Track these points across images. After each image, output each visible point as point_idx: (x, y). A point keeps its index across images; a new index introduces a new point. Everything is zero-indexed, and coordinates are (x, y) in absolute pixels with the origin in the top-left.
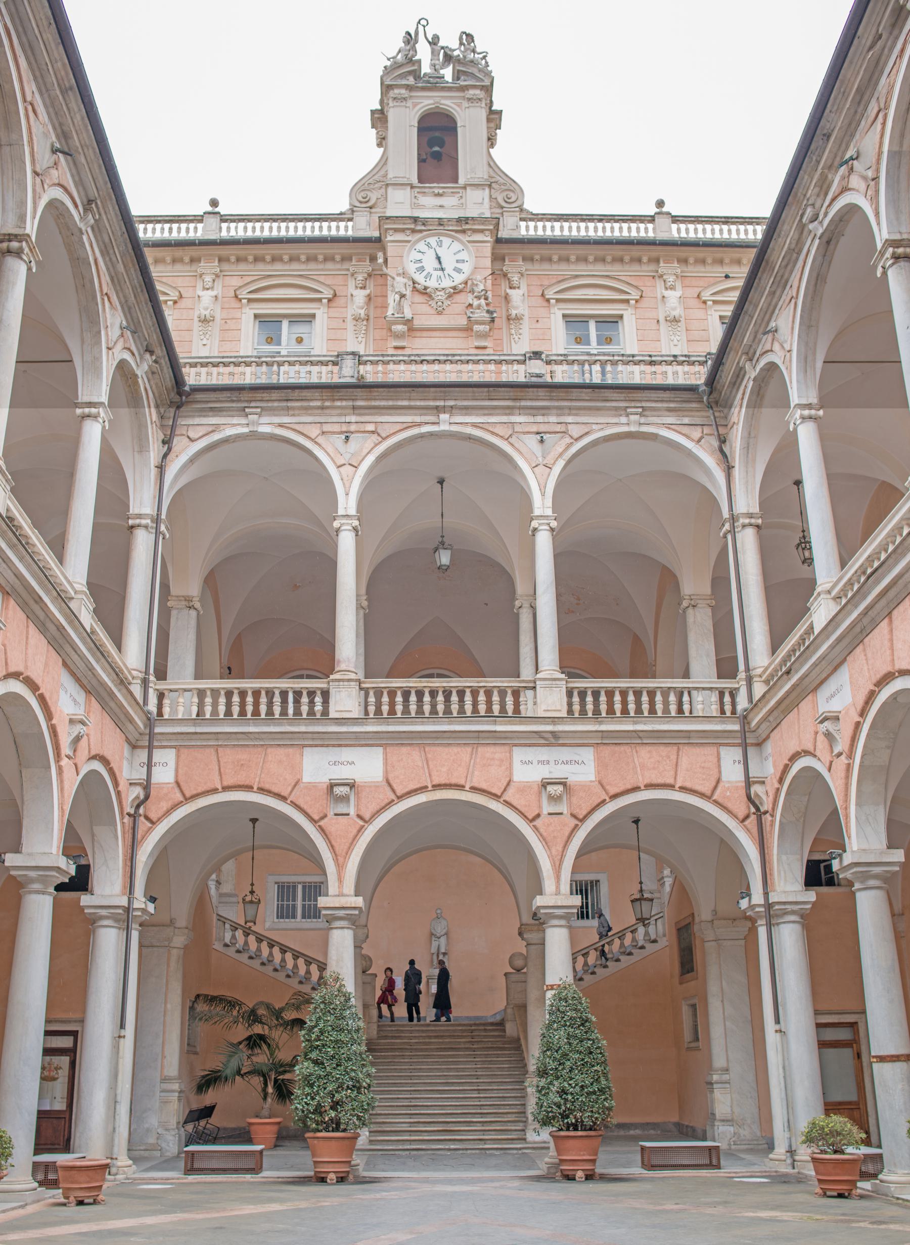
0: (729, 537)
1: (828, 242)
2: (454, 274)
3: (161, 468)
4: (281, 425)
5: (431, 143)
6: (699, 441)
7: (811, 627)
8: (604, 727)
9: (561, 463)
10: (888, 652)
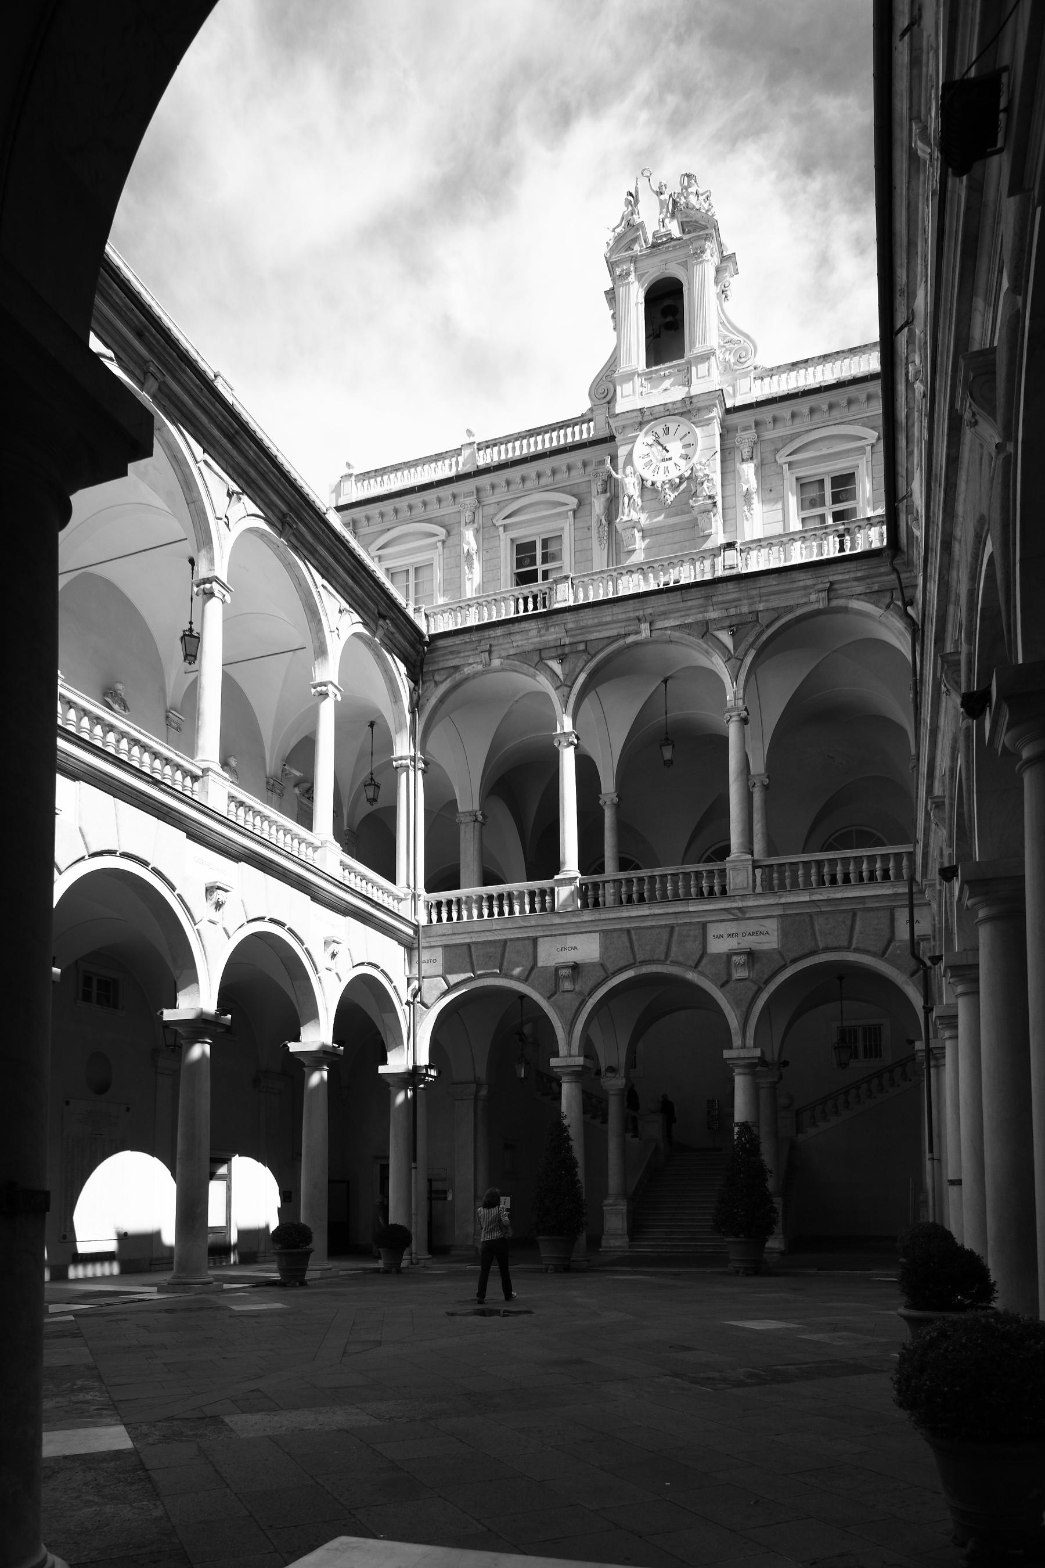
8: (783, 900)
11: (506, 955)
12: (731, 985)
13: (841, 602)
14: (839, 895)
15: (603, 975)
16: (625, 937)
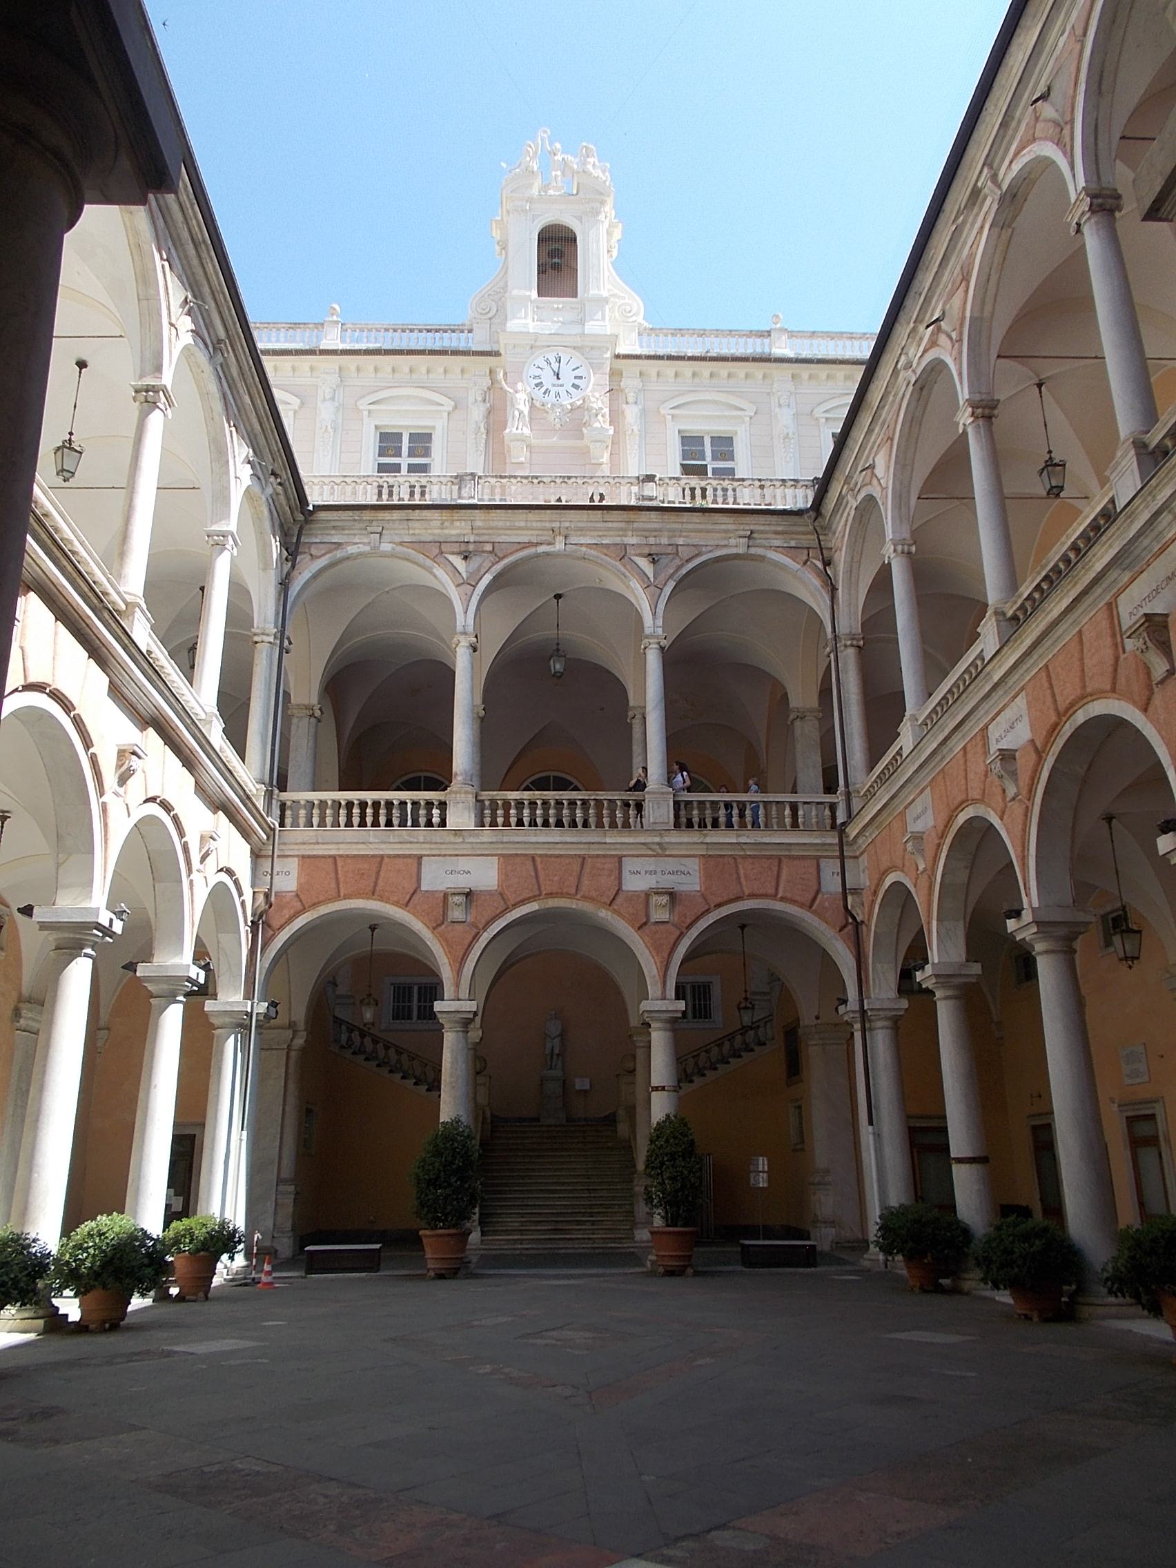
0: (832, 656)
1: (921, 389)
2: (572, 390)
3: (284, 584)
4: (401, 543)
5: (552, 254)
6: (805, 563)
7: (899, 753)
8: (708, 840)
9: (671, 584)
10: (963, 782)
11: (382, 874)
12: (646, 929)
13: (760, 551)
14: (767, 840)
15: (502, 906)
16: (529, 863)
